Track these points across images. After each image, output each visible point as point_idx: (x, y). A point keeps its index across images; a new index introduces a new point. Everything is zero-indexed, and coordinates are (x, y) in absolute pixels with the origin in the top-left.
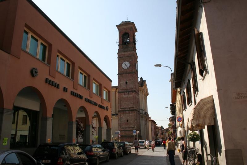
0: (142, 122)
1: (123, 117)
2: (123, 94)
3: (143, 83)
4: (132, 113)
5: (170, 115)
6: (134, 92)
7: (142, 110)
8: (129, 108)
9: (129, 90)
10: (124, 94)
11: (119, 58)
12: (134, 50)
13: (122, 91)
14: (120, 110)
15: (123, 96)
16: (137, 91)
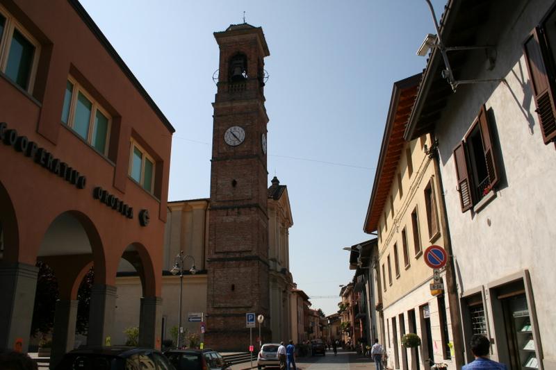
0: (275, 295)
1: (221, 277)
2: (223, 212)
3: (279, 191)
4: (245, 266)
5: (349, 276)
6: (255, 209)
7: (274, 260)
8: (240, 252)
10: (227, 215)
11: (218, 116)
12: (257, 98)
13: (222, 205)
14: (215, 256)
15: (224, 218)
16: (260, 205)
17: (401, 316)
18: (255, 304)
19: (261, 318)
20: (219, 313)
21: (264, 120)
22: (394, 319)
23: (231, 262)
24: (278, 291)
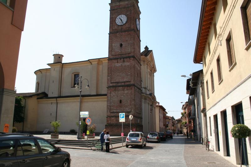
0: (145, 107)
1: (114, 96)
2: (116, 61)
3: (148, 52)
4: (127, 90)
5: (186, 98)
6: (133, 58)
7: (145, 88)
8: (124, 82)
9: (125, 56)
10: (117, 62)
11: (112, 10)
14: (111, 85)
16: (135, 56)
17: (224, 113)
18: (133, 110)
19: (131, 117)
20: (113, 115)
21: (139, 13)
22: (216, 117)
23: (120, 88)
24: (147, 105)
